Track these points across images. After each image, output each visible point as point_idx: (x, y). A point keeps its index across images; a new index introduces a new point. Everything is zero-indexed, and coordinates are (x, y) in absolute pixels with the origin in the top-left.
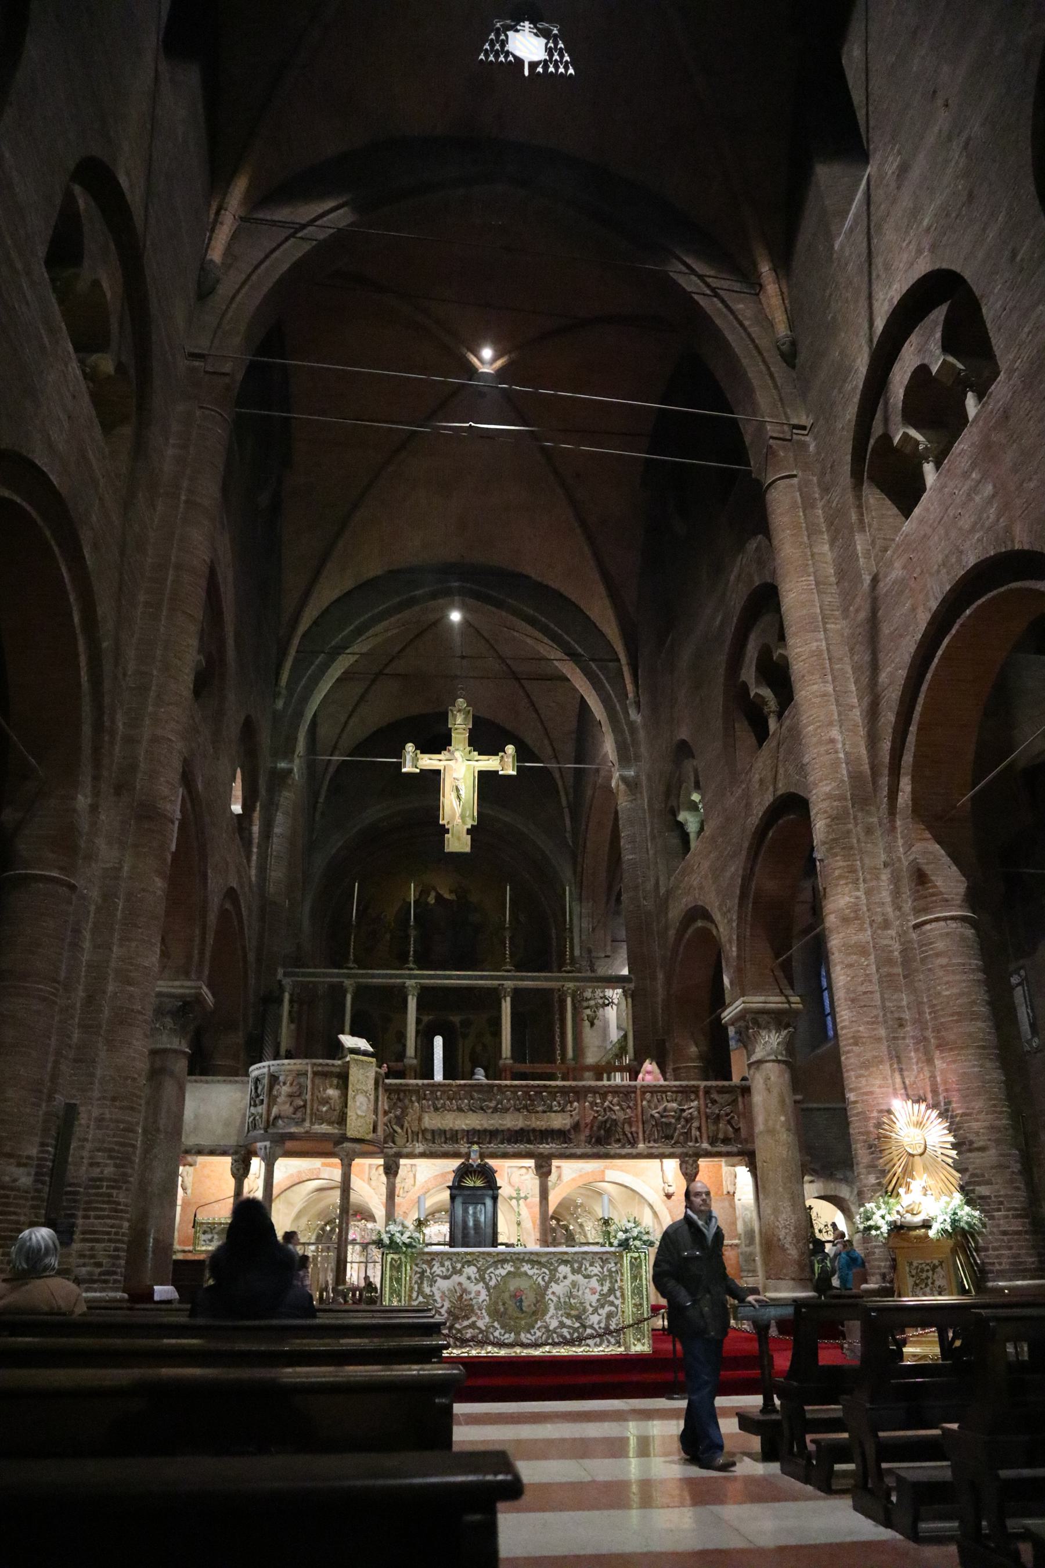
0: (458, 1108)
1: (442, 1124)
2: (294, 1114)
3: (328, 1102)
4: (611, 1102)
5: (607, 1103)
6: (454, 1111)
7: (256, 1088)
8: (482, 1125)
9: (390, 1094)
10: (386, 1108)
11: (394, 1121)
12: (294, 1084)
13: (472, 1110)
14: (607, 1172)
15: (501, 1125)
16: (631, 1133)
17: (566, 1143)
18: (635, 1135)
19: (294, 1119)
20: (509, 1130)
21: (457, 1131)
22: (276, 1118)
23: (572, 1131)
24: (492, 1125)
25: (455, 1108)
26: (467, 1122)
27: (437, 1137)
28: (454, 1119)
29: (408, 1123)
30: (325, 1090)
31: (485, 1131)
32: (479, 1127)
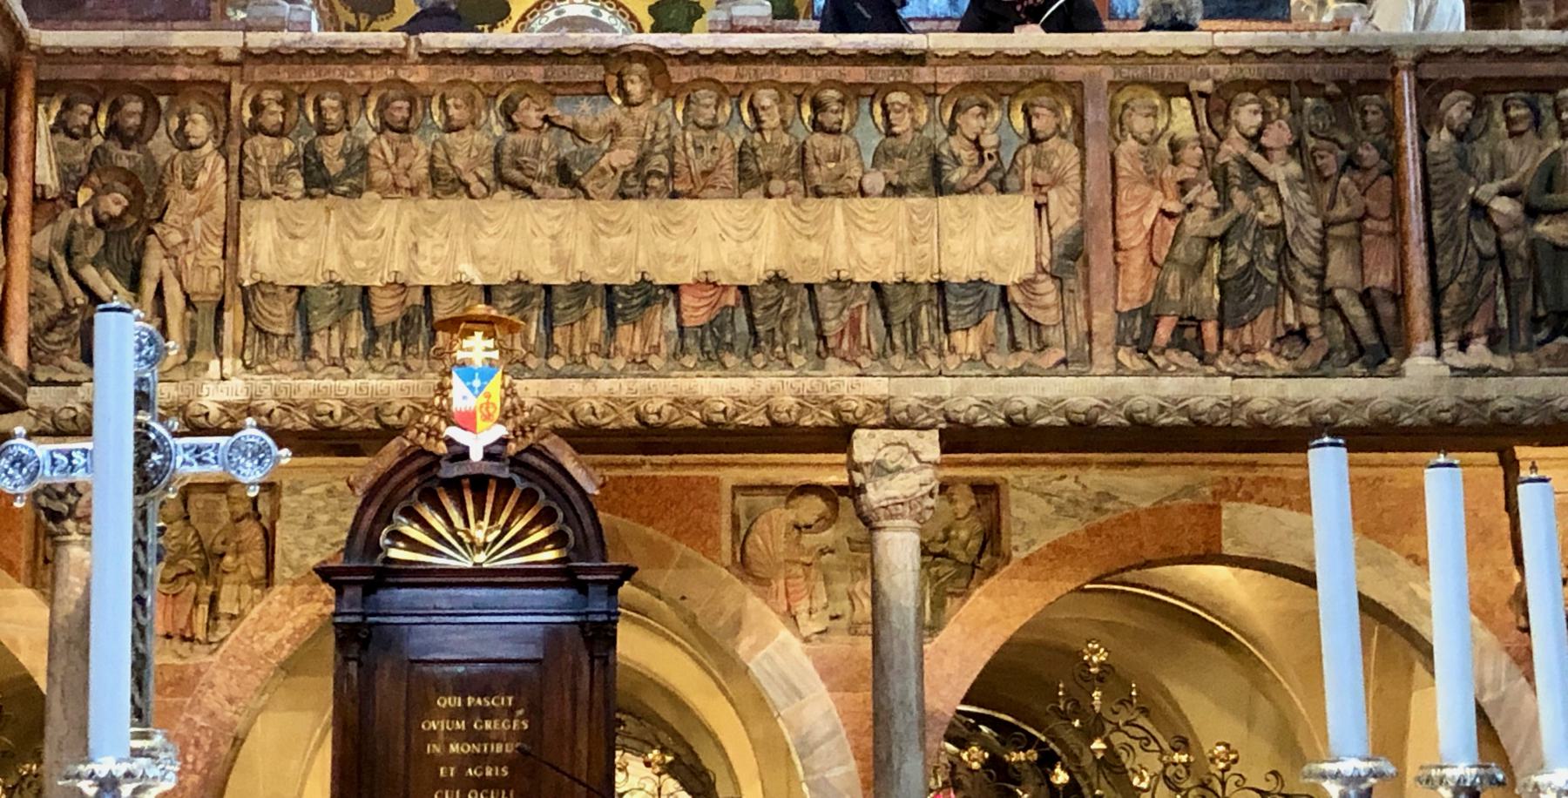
0: (434, 175)
1: (344, 251)
4: (1255, 140)
5: (1234, 147)
6: (414, 191)
8: (562, 261)
9: (67, 106)
10: (48, 176)
11: (94, 247)
13: (503, 181)
14: (1229, 511)
15: (662, 257)
16: (1366, 297)
17: (1015, 346)
18: (1387, 309)
20: (708, 283)
21: (427, 290)
23: (1047, 286)
24: (616, 259)
25: (421, 169)
26: (485, 244)
27: (320, 321)
28: (413, 229)
29: (169, 253)
31: (581, 289)
32: (544, 272)
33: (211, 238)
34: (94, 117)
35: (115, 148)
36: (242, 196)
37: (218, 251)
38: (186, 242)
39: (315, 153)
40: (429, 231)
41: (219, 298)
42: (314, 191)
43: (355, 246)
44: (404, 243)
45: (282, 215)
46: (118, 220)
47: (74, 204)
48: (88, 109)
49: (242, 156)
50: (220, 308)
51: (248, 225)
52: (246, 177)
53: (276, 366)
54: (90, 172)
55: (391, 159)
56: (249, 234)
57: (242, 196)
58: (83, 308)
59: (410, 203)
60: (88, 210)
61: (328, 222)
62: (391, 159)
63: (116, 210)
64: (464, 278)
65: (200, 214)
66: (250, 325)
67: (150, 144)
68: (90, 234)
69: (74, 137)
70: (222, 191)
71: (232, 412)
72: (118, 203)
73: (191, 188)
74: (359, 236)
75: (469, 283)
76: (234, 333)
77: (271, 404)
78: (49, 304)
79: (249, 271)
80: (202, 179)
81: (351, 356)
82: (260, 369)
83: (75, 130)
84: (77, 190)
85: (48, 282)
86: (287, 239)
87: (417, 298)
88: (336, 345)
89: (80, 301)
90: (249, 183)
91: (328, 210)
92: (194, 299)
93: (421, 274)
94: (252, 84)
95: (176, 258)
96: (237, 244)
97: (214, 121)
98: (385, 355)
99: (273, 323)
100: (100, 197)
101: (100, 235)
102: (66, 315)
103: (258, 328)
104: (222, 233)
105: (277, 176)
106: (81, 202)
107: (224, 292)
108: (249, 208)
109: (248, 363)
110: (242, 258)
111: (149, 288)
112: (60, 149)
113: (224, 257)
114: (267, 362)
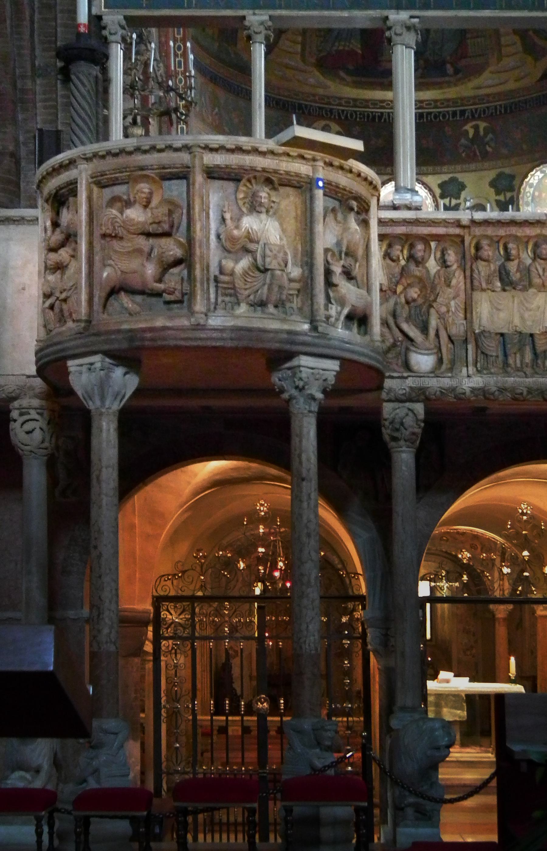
3: (247, 251)
7: (55, 225)
9: (390, 246)
11: (404, 312)
12: (155, 202)
19: (158, 294)
22: (113, 292)
29: (441, 317)
30: (237, 220)
33: (459, 309)
34: (402, 251)
35: (412, 267)
36: (472, 289)
37: (462, 315)
38: (448, 311)
39: (505, 269)
41: (464, 338)
46: (414, 300)
47: (395, 292)
48: (399, 247)
49: (472, 271)
51: (476, 303)
54: (401, 278)
55: (541, 273)
56: (477, 308)
57: (472, 289)
58: (402, 342)
60: (402, 297)
61: (513, 302)
62: (541, 273)
63: (415, 296)
65: (454, 298)
67: (427, 265)
68: (403, 307)
69: (393, 261)
70: (463, 288)
71: (476, 392)
72: (416, 293)
73: (449, 286)
76: (473, 355)
78: (387, 340)
79: (477, 326)
80: (454, 282)
81: (527, 366)
82: (485, 372)
83: (394, 258)
84: (396, 286)
85: (386, 330)
86: (495, 310)
88: (518, 362)
89: (400, 339)
90: (476, 283)
91: (513, 297)
92: (453, 338)
94: (475, 236)
95: (444, 319)
96: (472, 313)
97: (456, 254)
98: (542, 366)
99: (490, 350)
100: (407, 290)
101: (407, 307)
102: (394, 345)
103: (483, 353)
104: (463, 307)
105: (489, 281)
106: (398, 292)
107: (467, 335)
108: (477, 295)
111: (432, 333)
112: (386, 268)
113: (466, 319)
114: (487, 369)
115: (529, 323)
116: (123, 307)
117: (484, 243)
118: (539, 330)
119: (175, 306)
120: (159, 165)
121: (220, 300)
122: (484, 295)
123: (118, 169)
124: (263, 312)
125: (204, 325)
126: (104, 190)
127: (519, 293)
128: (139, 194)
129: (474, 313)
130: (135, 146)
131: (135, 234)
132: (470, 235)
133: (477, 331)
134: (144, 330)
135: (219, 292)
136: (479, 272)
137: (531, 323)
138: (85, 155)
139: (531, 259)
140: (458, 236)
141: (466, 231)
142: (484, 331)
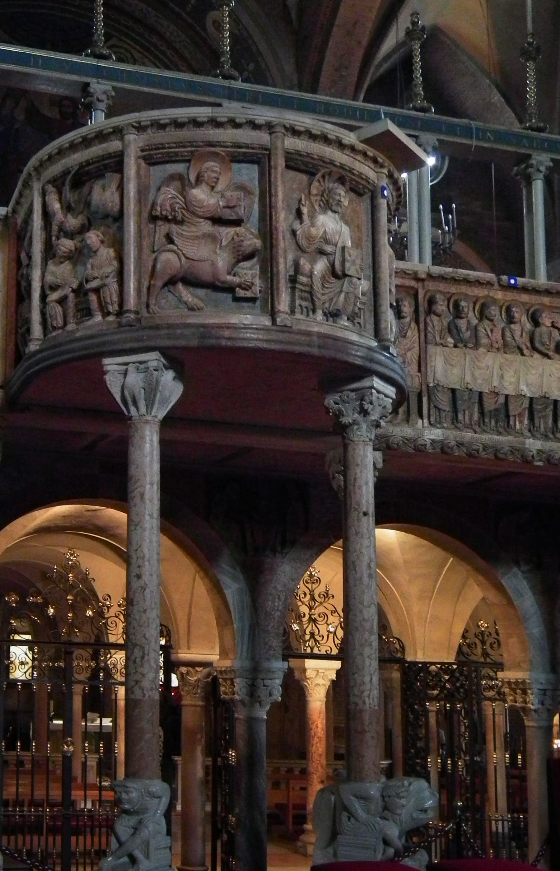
1: (473, 375)
2: (229, 273)
19: (230, 289)
21: (507, 396)
40: (508, 369)
42: (460, 345)
43: (477, 373)
44: (498, 374)
45: (445, 354)
50: (420, 396)
51: (431, 356)
52: (429, 334)
53: (445, 425)
56: (431, 361)
57: (426, 342)
59: (499, 355)
61: (465, 359)
64: (523, 394)
65: (409, 350)
66: (432, 405)
74: (479, 368)
75: (524, 395)
77: (453, 443)
80: (409, 333)
87: (502, 400)
88: (467, 418)
90: (430, 337)
93: (506, 389)
103: (435, 407)
107: (421, 387)
108: (431, 349)
109: (432, 422)
110: (429, 373)
113: (419, 371)
114: (440, 423)
115: (479, 381)
116: (180, 300)
117: (439, 298)
118: (489, 390)
119: (245, 304)
120: (235, 143)
121: (298, 302)
122: (439, 349)
123: (181, 142)
124: (334, 322)
125: (291, 327)
126: (151, 168)
127: (471, 351)
128: (209, 173)
129: (428, 366)
130: (209, 117)
131: (202, 218)
132: (423, 288)
133: (431, 385)
134: (219, 327)
135: (297, 293)
136: (433, 326)
137: (481, 382)
138: (139, 123)
139: (477, 318)
140: (412, 288)
141: (420, 284)
142: (438, 385)
